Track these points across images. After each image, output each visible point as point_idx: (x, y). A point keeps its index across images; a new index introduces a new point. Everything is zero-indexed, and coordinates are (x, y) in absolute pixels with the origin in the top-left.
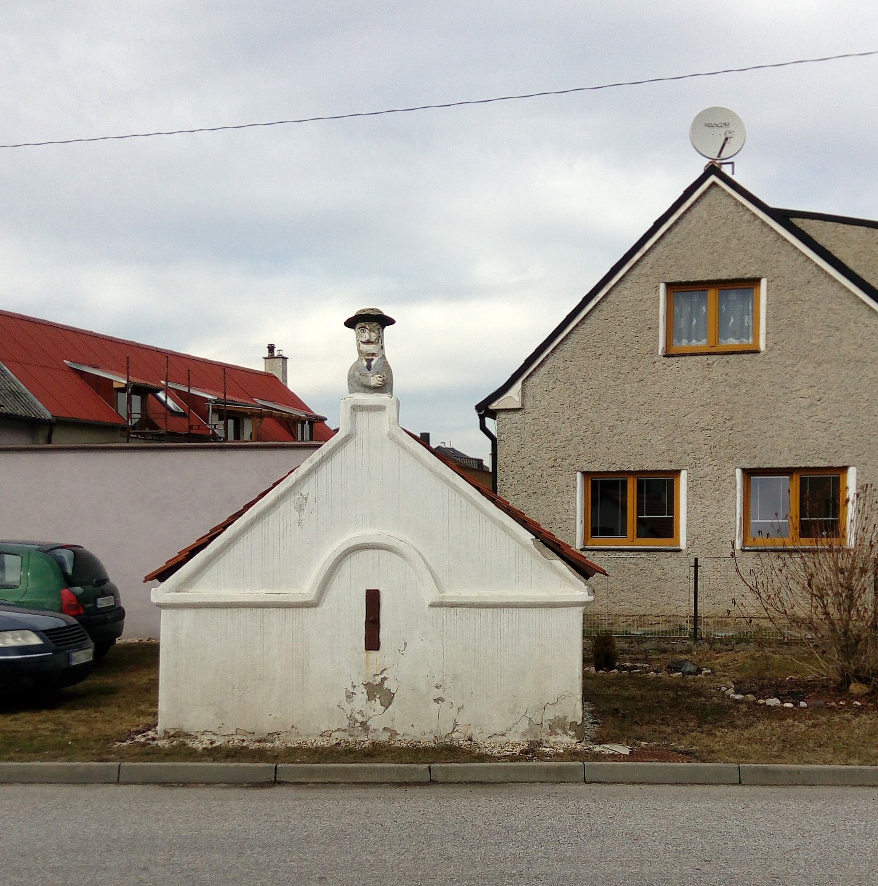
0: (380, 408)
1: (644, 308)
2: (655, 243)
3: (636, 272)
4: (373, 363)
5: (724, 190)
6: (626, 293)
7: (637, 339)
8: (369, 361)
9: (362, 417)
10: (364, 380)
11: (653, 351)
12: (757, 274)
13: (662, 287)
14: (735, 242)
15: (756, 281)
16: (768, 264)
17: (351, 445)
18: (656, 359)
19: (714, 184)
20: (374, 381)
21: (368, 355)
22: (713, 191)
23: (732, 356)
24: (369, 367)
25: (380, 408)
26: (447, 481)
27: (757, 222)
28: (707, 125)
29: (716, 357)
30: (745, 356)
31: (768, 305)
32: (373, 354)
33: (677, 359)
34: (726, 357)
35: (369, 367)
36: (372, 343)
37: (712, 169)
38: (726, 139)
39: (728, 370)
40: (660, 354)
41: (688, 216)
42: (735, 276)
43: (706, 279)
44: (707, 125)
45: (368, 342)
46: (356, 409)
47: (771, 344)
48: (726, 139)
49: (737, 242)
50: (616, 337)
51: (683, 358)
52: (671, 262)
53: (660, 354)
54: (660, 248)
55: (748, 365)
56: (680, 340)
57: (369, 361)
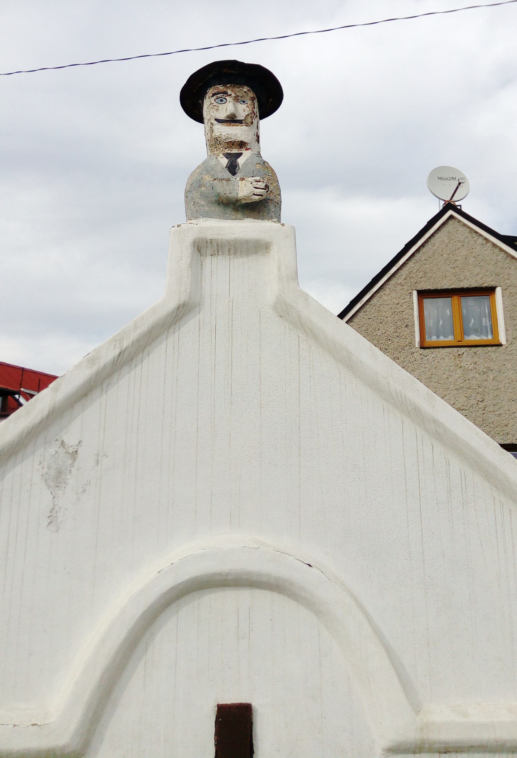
0: (258, 248)
1: (401, 309)
2: (407, 260)
3: (393, 282)
4: (241, 161)
5: (459, 221)
6: (385, 298)
7: (397, 334)
8: (232, 159)
9: (217, 268)
10: (224, 189)
11: (411, 344)
12: (493, 284)
13: (415, 293)
14: (471, 260)
15: (490, 291)
16: (501, 276)
17: (189, 327)
18: (414, 350)
19: (451, 217)
20: (245, 189)
21: (232, 144)
22: (451, 222)
23: (478, 349)
24: (233, 168)
25: (258, 248)
26: (415, 414)
27: (489, 244)
28: (440, 178)
29: (465, 349)
30: (489, 348)
31: (505, 308)
32: (242, 144)
33: (432, 350)
34: (474, 350)
35: (233, 168)
36: (240, 122)
37: (449, 206)
38: (460, 184)
39: (476, 359)
40: (417, 346)
41: (432, 241)
42: (474, 285)
43: (451, 287)
44: (440, 178)
45: (232, 120)
46: (203, 248)
47: (510, 339)
48: (460, 184)
49: (474, 259)
50: (379, 333)
51: (437, 350)
52: (421, 274)
53: (417, 346)
54: (411, 264)
55: (493, 355)
56: (430, 337)
57: (232, 159)
